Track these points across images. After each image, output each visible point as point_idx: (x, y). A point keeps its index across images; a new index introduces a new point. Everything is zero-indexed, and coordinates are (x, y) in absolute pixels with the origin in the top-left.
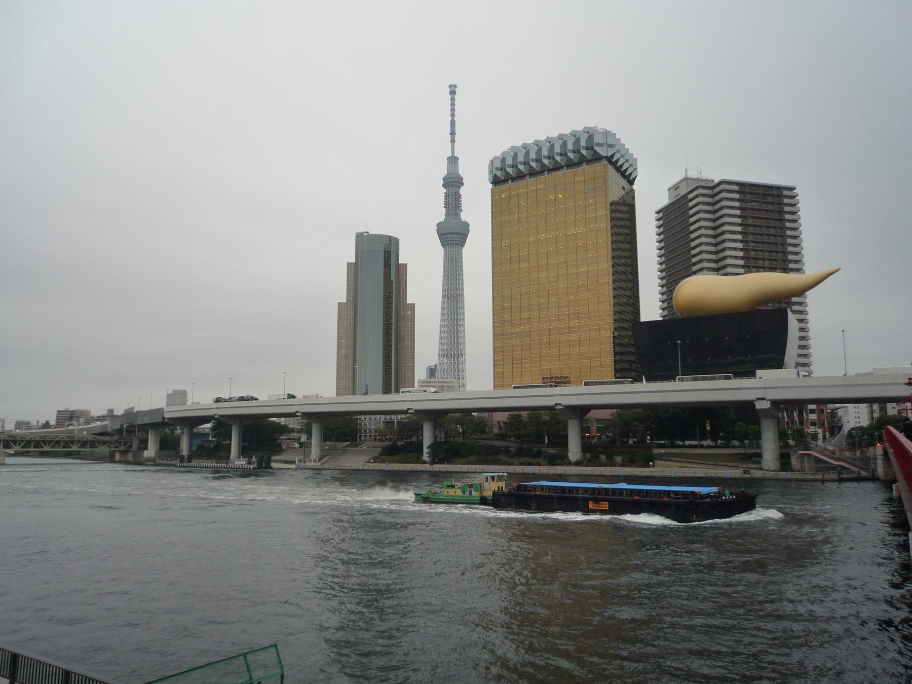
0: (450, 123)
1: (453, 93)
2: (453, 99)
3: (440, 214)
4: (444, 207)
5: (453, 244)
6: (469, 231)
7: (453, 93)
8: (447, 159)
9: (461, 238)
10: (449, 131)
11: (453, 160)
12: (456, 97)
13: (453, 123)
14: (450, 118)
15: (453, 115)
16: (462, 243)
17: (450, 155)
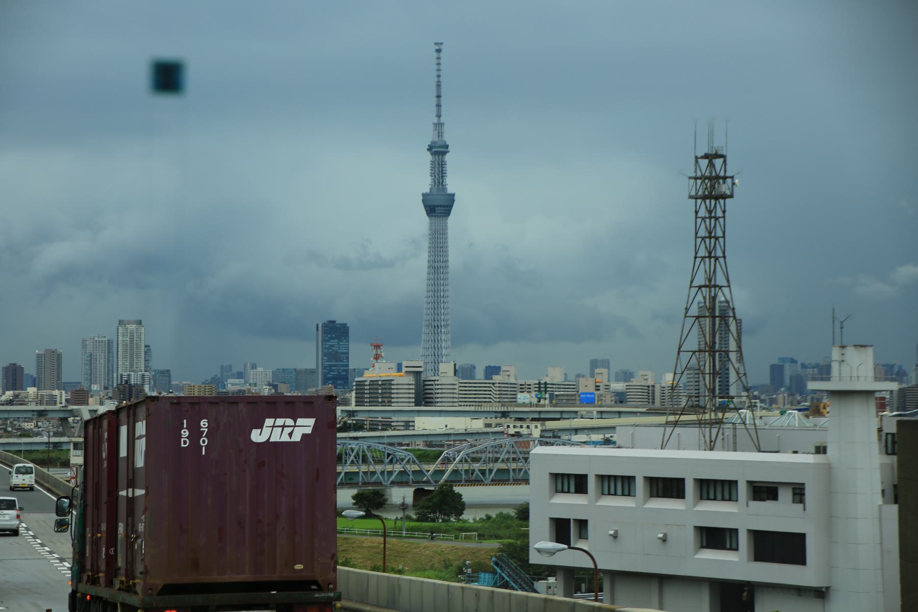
0: (435, 84)
1: (439, 51)
2: (439, 58)
3: (425, 184)
4: (431, 176)
5: (438, 216)
6: (454, 200)
7: (439, 51)
8: (434, 124)
9: (446, 210)
10: (435, 94)
11: (439, 126)
12: (442, 54)
13: (439, 85)
14: (436, 79)
15: (439, 76)
16: (448, 213)
17: (435, 120)
